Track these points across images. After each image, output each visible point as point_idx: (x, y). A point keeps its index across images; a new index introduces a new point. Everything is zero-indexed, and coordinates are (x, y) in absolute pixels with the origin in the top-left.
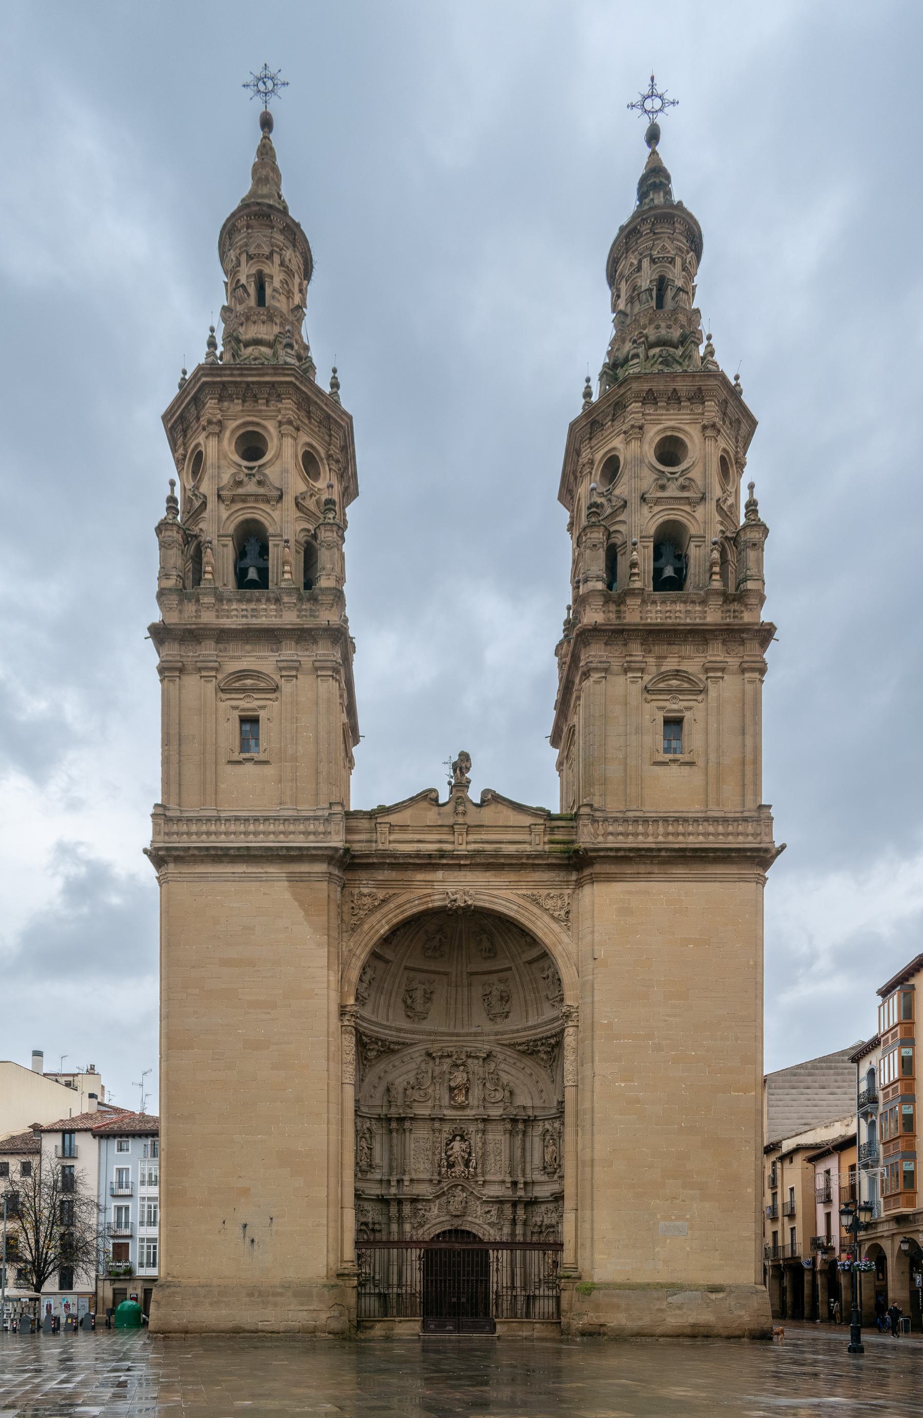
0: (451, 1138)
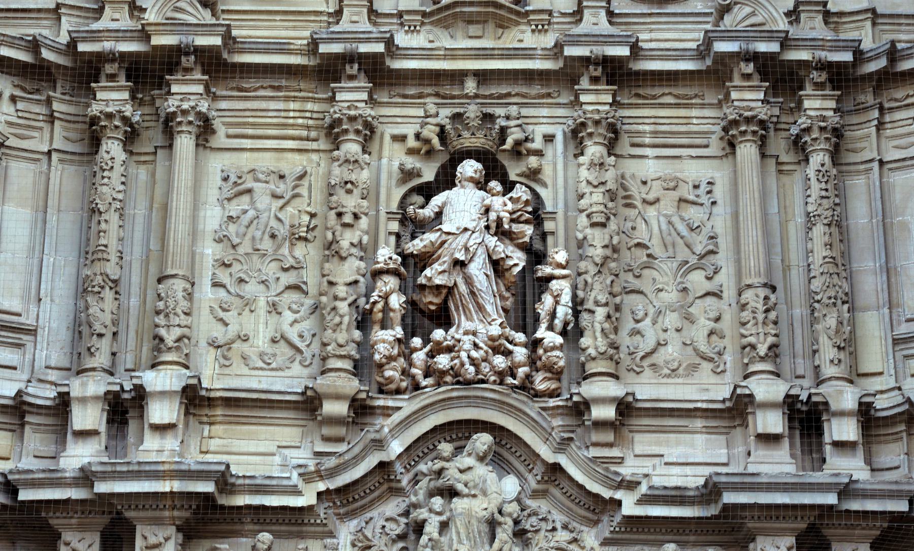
0: (429, 174)
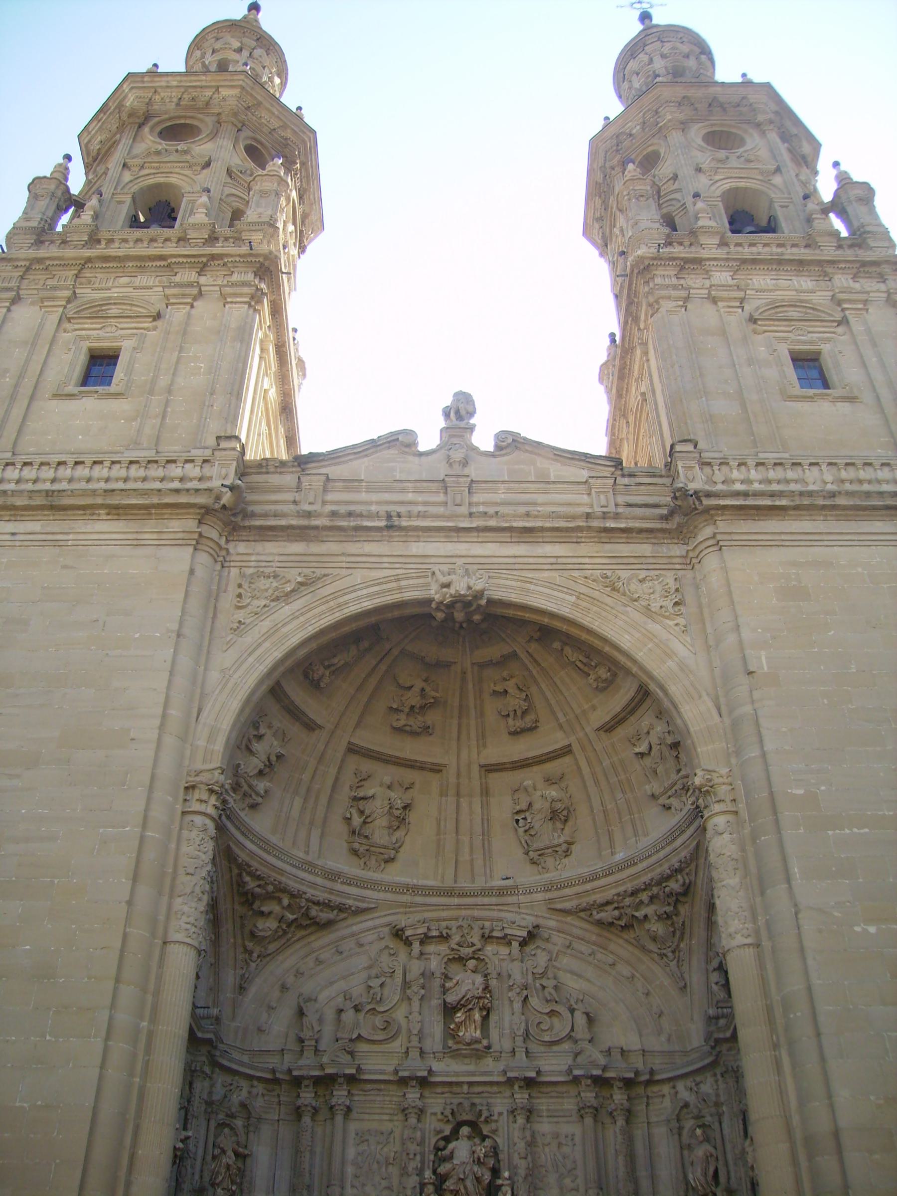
0: (447, 1132)
